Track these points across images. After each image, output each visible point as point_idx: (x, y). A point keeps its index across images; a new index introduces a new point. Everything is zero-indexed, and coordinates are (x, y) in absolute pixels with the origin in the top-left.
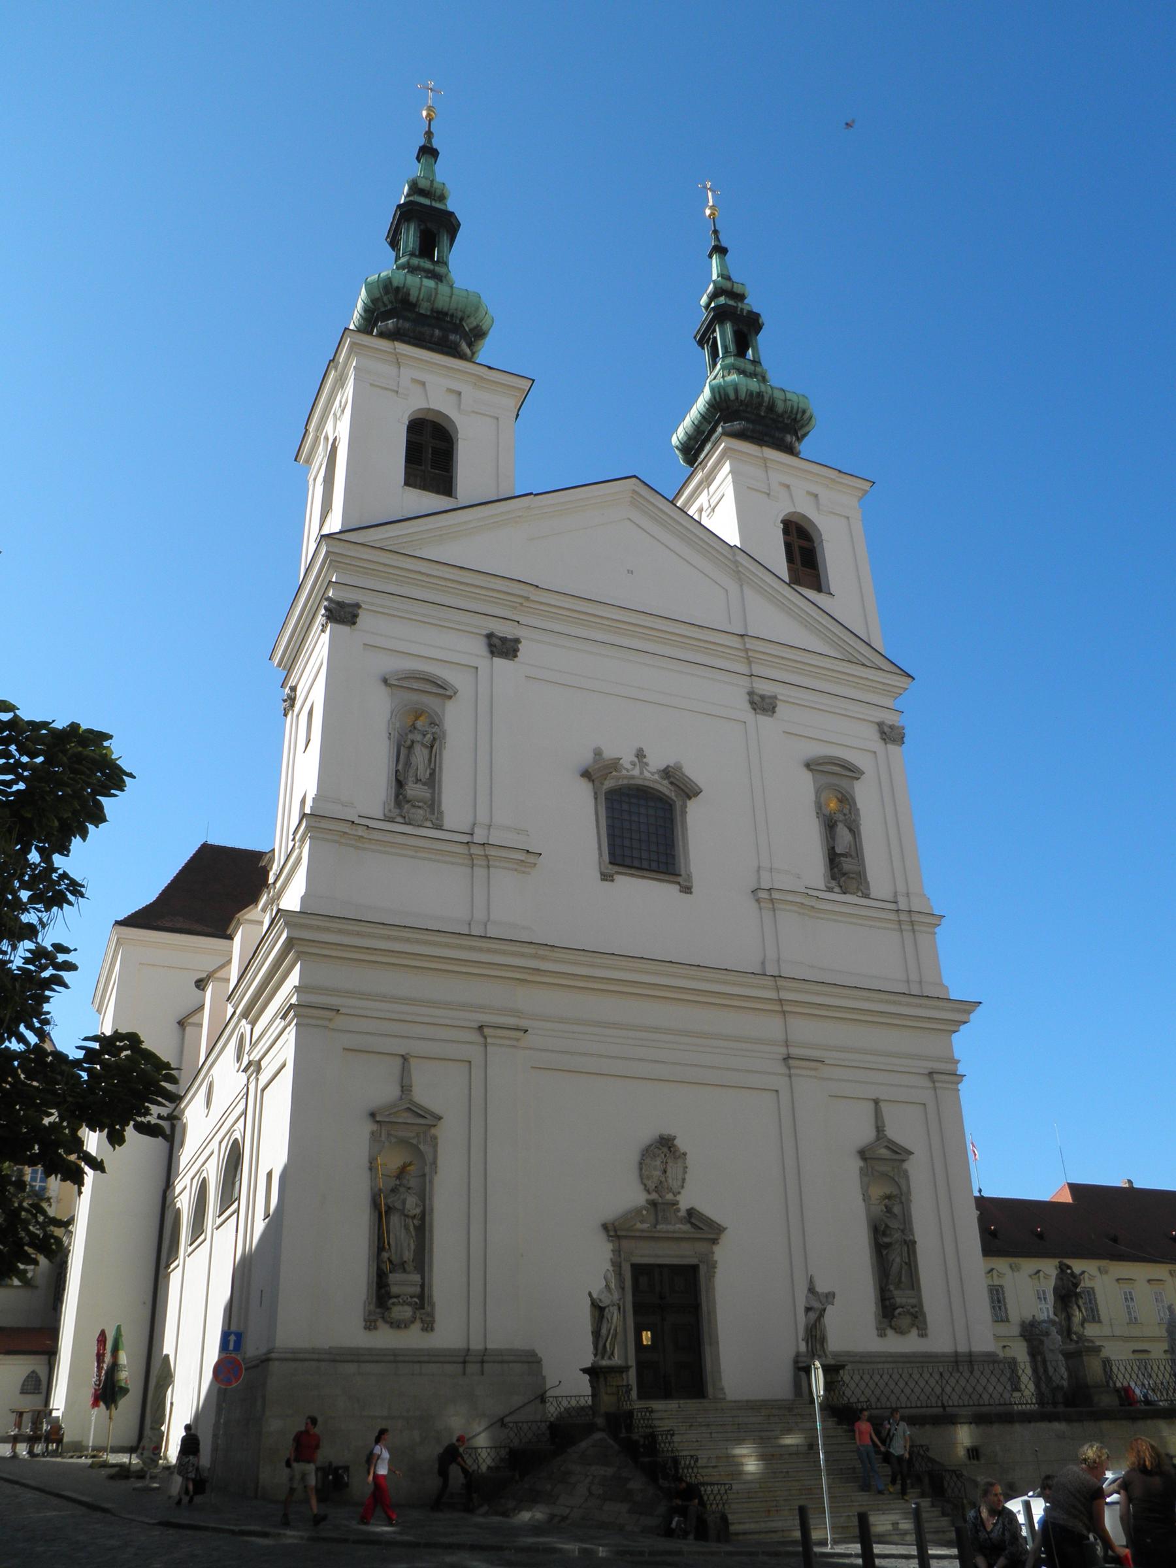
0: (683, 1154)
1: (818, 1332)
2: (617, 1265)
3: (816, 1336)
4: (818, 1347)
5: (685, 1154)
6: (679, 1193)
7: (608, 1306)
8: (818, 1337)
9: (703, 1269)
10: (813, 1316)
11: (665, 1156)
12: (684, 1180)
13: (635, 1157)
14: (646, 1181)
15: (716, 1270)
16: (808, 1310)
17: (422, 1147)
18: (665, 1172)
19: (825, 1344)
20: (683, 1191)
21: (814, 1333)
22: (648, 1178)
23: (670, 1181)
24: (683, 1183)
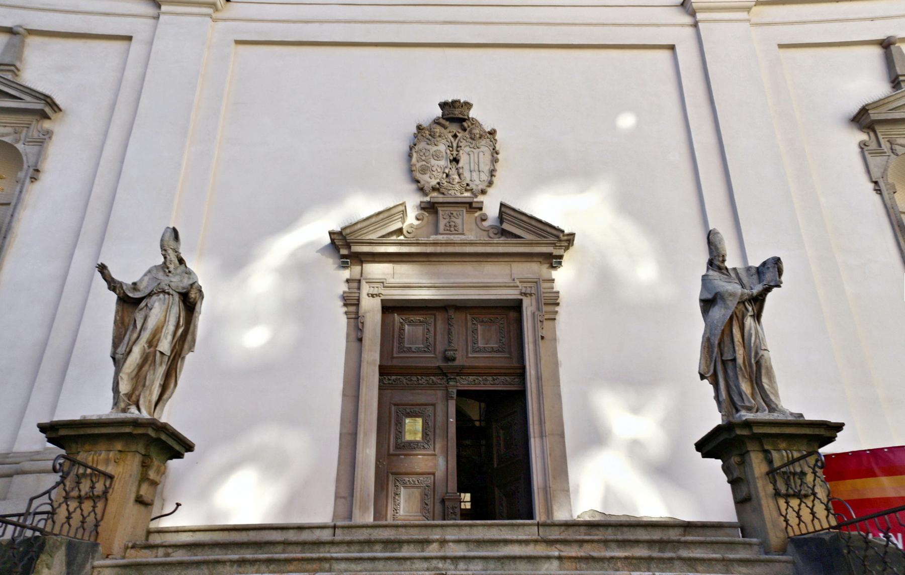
0: (490, 133)
1: (740, 353)
2: (351, 302)
3: (734, 360)
4: (745, 387)
5: (492, 133)
6: (483, 192)
7: (150, 295)
8: (740, 361)
9: (528, 307)
10: (719, 313)
11: (455, 136)
12: (492, 173)
13: (402, 147)
14: (418, 176)
15: (557, 309)
16: (707, 304)
17: (20, 146)
18: (456, 160)
19: (765, 381)
20: (490, 191)
21: (728, 356)
22: (424, 171)
23: (466, 175)
24: (492, 176)
